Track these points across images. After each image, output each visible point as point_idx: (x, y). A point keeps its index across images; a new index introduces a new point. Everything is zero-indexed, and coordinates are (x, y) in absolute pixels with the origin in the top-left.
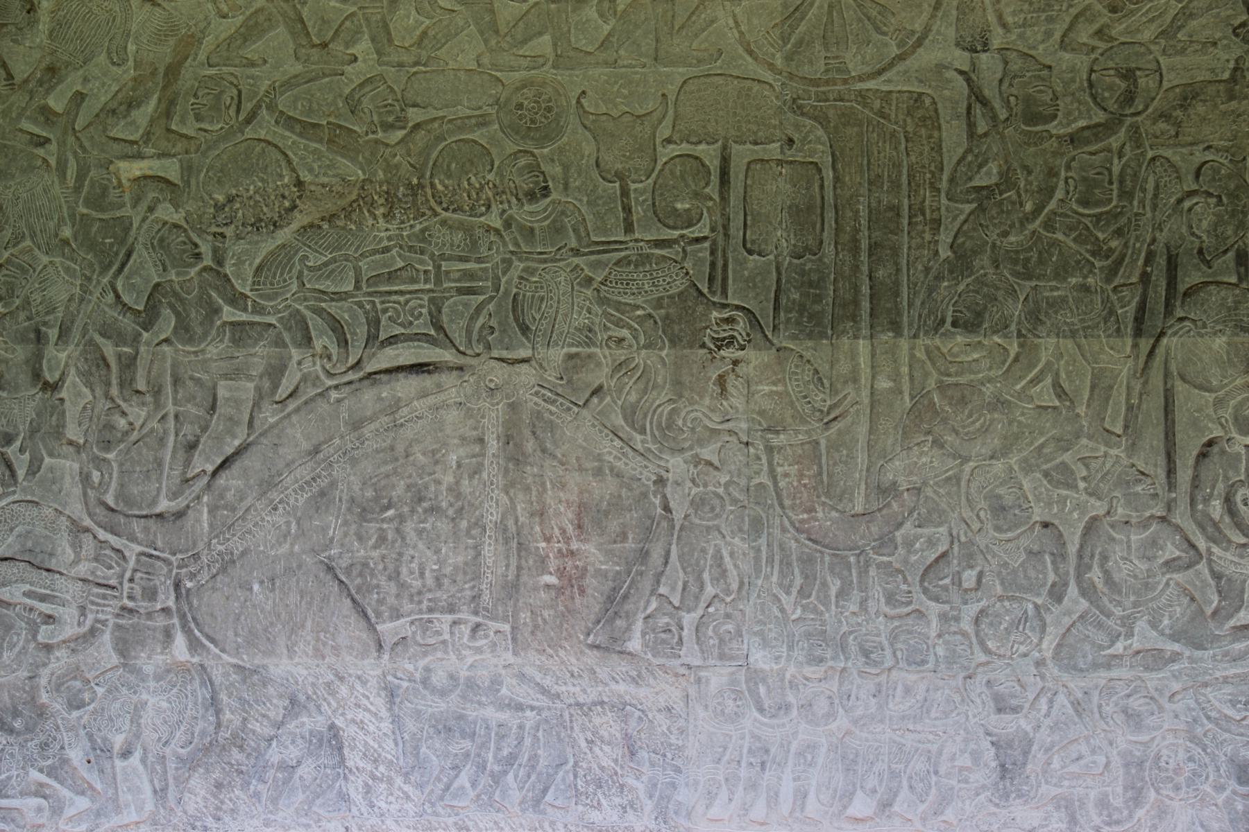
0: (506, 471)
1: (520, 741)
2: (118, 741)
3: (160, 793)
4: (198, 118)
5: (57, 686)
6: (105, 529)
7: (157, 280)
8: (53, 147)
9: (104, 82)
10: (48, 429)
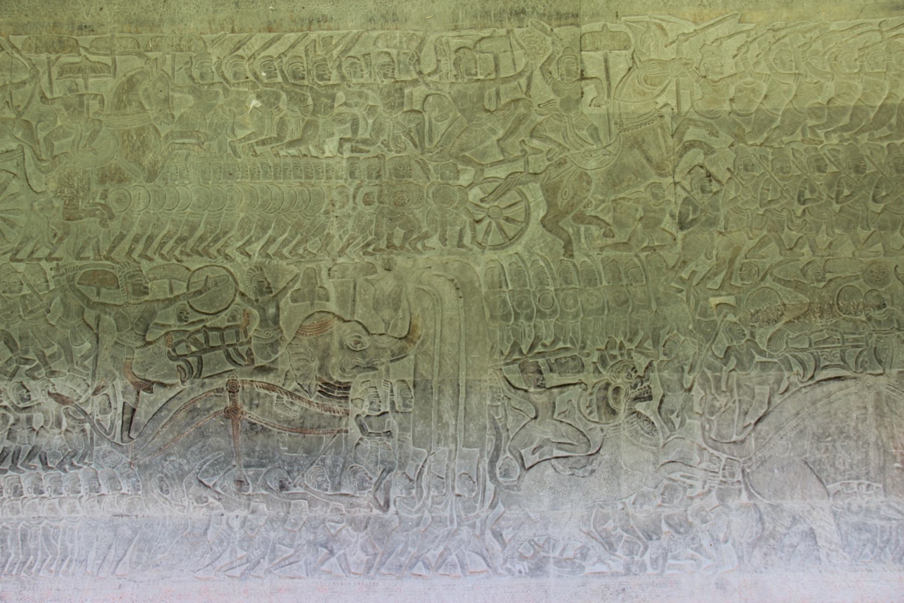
0: (877, 421)
1: (891, 534)
2: (721, 536)
3: (740, 558)
4: (742, 279)
5: (697, 514)
6: (713, 448)
7: (727, 345)
8: (684, 293)
9: (702, 266)
10: (687, 408)
